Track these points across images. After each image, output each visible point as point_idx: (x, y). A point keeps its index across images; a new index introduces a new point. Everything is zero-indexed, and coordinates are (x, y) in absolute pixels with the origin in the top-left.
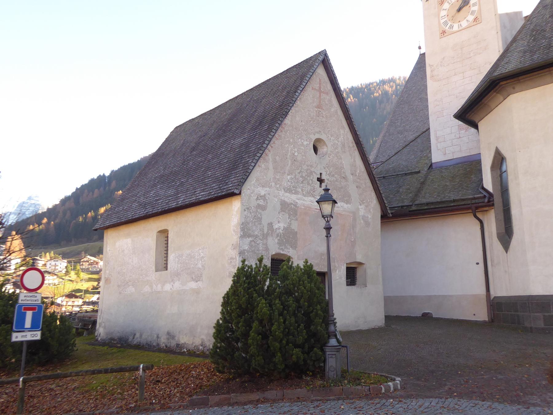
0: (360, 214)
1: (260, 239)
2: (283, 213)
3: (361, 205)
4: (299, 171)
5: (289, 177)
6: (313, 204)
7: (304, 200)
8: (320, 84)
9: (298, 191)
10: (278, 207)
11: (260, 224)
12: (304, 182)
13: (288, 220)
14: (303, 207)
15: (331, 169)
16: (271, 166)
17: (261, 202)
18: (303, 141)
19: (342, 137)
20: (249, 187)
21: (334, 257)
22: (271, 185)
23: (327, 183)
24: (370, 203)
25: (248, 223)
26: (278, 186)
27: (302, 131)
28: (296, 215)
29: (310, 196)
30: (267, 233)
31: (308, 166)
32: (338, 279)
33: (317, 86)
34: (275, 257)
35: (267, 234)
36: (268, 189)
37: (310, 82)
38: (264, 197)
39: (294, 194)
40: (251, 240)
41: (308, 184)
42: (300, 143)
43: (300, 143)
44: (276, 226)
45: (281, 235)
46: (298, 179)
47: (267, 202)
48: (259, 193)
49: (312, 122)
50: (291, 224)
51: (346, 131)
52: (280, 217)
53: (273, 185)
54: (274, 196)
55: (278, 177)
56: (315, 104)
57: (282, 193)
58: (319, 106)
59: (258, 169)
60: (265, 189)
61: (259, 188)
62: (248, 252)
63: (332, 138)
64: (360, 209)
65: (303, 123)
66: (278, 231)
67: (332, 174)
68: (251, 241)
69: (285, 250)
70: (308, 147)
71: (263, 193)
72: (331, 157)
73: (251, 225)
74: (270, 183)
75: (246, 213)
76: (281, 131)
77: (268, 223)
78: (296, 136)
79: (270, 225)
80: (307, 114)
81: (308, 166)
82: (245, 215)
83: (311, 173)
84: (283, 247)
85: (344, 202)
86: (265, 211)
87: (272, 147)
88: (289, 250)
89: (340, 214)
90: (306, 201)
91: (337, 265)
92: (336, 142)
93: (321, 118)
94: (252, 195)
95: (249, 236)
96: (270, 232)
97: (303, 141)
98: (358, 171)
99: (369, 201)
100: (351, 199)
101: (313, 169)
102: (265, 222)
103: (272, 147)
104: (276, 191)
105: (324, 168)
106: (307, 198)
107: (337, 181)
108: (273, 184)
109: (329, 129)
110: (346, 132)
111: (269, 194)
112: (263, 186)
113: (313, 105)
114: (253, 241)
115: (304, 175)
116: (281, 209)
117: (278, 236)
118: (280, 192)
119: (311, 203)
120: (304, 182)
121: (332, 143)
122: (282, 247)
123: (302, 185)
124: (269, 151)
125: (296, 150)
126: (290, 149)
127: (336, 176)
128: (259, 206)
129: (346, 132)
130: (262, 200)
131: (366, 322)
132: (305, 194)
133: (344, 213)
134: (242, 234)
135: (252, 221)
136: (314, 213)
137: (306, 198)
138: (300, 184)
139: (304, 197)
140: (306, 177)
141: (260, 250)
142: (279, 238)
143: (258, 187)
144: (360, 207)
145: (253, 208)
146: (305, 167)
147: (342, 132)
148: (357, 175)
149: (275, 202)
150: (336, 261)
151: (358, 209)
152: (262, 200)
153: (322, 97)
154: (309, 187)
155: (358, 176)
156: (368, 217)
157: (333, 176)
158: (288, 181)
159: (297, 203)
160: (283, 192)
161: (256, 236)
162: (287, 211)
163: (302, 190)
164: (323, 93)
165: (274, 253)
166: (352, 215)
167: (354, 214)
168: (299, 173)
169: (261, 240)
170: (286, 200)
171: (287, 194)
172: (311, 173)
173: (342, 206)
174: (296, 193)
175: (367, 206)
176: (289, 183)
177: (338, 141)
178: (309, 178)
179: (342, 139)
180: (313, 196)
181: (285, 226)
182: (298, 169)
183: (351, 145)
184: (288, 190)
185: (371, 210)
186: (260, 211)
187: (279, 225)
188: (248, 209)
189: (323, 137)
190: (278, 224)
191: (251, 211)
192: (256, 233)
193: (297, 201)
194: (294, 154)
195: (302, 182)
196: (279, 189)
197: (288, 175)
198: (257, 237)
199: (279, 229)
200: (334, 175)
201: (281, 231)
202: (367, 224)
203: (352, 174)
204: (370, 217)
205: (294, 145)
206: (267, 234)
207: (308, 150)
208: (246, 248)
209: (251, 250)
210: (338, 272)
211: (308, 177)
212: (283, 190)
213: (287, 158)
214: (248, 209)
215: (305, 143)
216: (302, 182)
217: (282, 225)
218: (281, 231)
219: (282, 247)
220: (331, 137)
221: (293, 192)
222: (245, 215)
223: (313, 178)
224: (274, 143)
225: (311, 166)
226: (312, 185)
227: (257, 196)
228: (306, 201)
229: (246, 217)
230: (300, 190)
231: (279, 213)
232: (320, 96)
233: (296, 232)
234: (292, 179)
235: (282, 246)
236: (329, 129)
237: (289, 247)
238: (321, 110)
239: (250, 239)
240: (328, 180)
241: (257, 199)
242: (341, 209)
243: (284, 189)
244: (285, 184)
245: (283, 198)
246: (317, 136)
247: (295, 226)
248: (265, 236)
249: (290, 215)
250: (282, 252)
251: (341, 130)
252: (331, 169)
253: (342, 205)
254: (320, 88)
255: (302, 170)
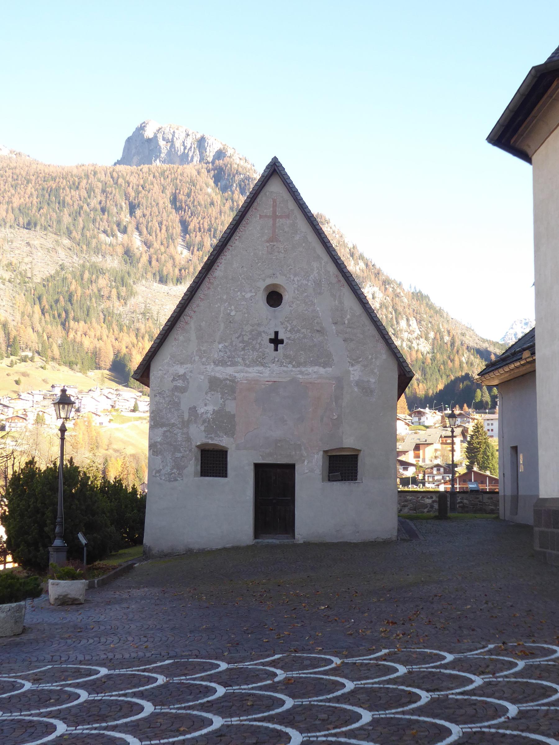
0: (352, 379)
1: (178, 428)
2: (213, 393)
3: (353, 365)
4: (237, 335)
5: (220, 346)
6: (261, 375)
7: (246, 372)
8: (274, 206)
9: (237, 362)
10: (206, 385)
11: (178, 410)
12: (246, 348)
13: (221, 401)
14: (246, 382)
15: (295, 323)
16: (193, 335)
17: (180, 383)
18: (243, 294)
19: (315, 272)
20: (160, 368)
21: (299, 443)
22: (194, 360)
23: (287, 343)
24: (374, 360)
25: (161, 411)
26: (204, 360)
27: (243, 281)
28: (235, 393)
29: (257, 365)
30: (188, 419)
31: (253, 326)
32: (307, 473)
33: (269, 211)
34: (207, 448)
35: (189, 421)
36: (189, 366)
37: (256, 209)
38: (183, 377)
39: (230, 366)
40: (166, 430)
41: (254, 349)
42: (239, 297)
43: (239, 297)
44: (201, 410)
45: (209, 421)
46: (236, 346)
47: (188, 383)
48: (177, 372)
49: (260, 264)
50: (225, 405)
51: (323, 262)
52: (207, 398)
53: (196, 360)
54: (199, 374)
55: (203, 349)
56: (265, 238)
57: (210, 367)
58: (273, 239)
59: (173, 344)
60: (185, 366)
61: (175, 367)
62: (161, 444)
63: (296, 279)
64: (352, 372)
65: (245, 269)
66: (205, 416)
67: (296, 329)
68: (165, 432)
69: (216, 438)
70: (253, 300)
71: (181, 371)
72: (294, 306)
73: (164, 412)
74: (192, 358)
75: (157, 399)
76: (209, 288)
77: (190, 408)
78: (233, 290)
79: (193, 410)
80: (252, 254)
81: (253, 326)
82: (156, 402)
83: (259, 334)
84: (213, 436)
85: (320, 366)
86: (184, 394)
87: (195, 312)
88: (221, 439)
89: (311, 383)
90: (250, 373)
91: (305, 454)
92: (305, 282)
93: (276, 254)
94: (166, 376)
95: (162, 425)
96: (192, 417)
97: (243, 294)
98: (348, 317)
99: (370, 357)
100: (333, 360)
101: (261, 329)
102: (185, 406)
103: (195, 312)
104: (202, 367)
105: (282, 324)
106: (251, 368)
107: (304, 337)
108: (197, 358)
109: (290, 267)
110: (323, 264)
111: (191, 372)
112: (182, 363)
113: (263, 240)
114: (168, 431)
115: (246, 338)
116: (210, 388)
117: (204, 421)
118: (208, 367)
119: (260, 375)
120: (246, 348)
121: (297, 286)
122: (210, 436)
123: (242, 353)
124: (191, 317)
125: (233, 307)
126: (222, 309)
127: (303, 331)
128: (176, 388)
129: (323, 264)
130: (181, 381)
131: (358, 532)
132: (248, 363)
133: (319, 381)
134: (152, 424)
135: (166, 407)
136: (263, 386)
137: (250, 370)
138: (241, 351)
139: (246, 368)
140: (250, 341)
141: (179, 441)
142: (206, 424)
143: (173, 366)
144: (351, 369)
145: (167, 391)
146: (248, 328)
147: (315, 265)
148: (346, 322)
149: (200, 380)
150: (303, 448)
151: (348, 372)
152: (181, 381)
153: (278, 225)
154: (256, 353)
155: (349, 323)
156: (368, 381)
157: (298, 331)
158: (220, 351)
159: (235, 377)
160: (212, 366)
161: (173, 425)
162: (219, 389)
163: (243, 359)
164: (281, 217)
165: (199, 443)
166: (334, 382)
167: (340, 382)
168: (238, 338)
169: (180, 429)
170: (218, 375)
171: (219, 368)
172: (259, 334)
173: (315, 372)
174: (234, 364)
175: (365, 366)
176: (222, 354)
177: (308, 281)
178: (254, 342)
179: (316, 275)
180: (262, 365)
181: (216, 408)
182: (237, 332)
183: (334, 280)
184: (217, 363)
185: (376, 371)
186: (178, 394)
187: (206, 408)
188: (159, 393)
189: (279, 280)
190: (205, 408)
191: (165, 396)
192: (173, 421)
193: (236, 374)
194: (229, 314)
195: (243, 349)
196: (207, 363)
197: (219, 343)
198: (173, 426)
199: (206, 413)
200: (300, 330)
201: (209, 415)
202: (366, 390)
203: (335, 323)
204: (373, 380)
205: (229, 303)
206: (189, 421)
207: (252, 304)
208: (159, 440)
209: (165, 442)
210: (308, 463)
211: (253, 340)
212: (212, 364)
213: (217, 322)
214: (159, 393)
215: (248, 295)
216: (243, 349)
217: (210, 408)
218: (209, 415)
219: (210, 436)
220: (295, 276)
221: (229, 363)
222: (156, 402)
223: (262, 340)
224: (198, 306)
225: (259, 325)
226: (260, 350)
227: (172, 377)
228: (250, 373)
229: (158, 403)
230: (240, 360)
231: (206, 393)
232: (274, 224)
233: (234, 416)
234: (226, 347)
235: (212, 434)
236: (290, 267)
237: (221, 434)
238: (275, 243)
239: (165, 429)
240: (289, 338)
241: (174, 380)
242: (314, 376)
243: (214, 363)
244: (216, 356)
245: (213, 374)
246: (269, 281)
247: (231, 407)
248: (185, 424)
249: (223, 394)
250: (210, 442)
251: (313, 263)
252: (295, 323)
253: (315, 370)
254: (274, 212)
255: (244, 333)
